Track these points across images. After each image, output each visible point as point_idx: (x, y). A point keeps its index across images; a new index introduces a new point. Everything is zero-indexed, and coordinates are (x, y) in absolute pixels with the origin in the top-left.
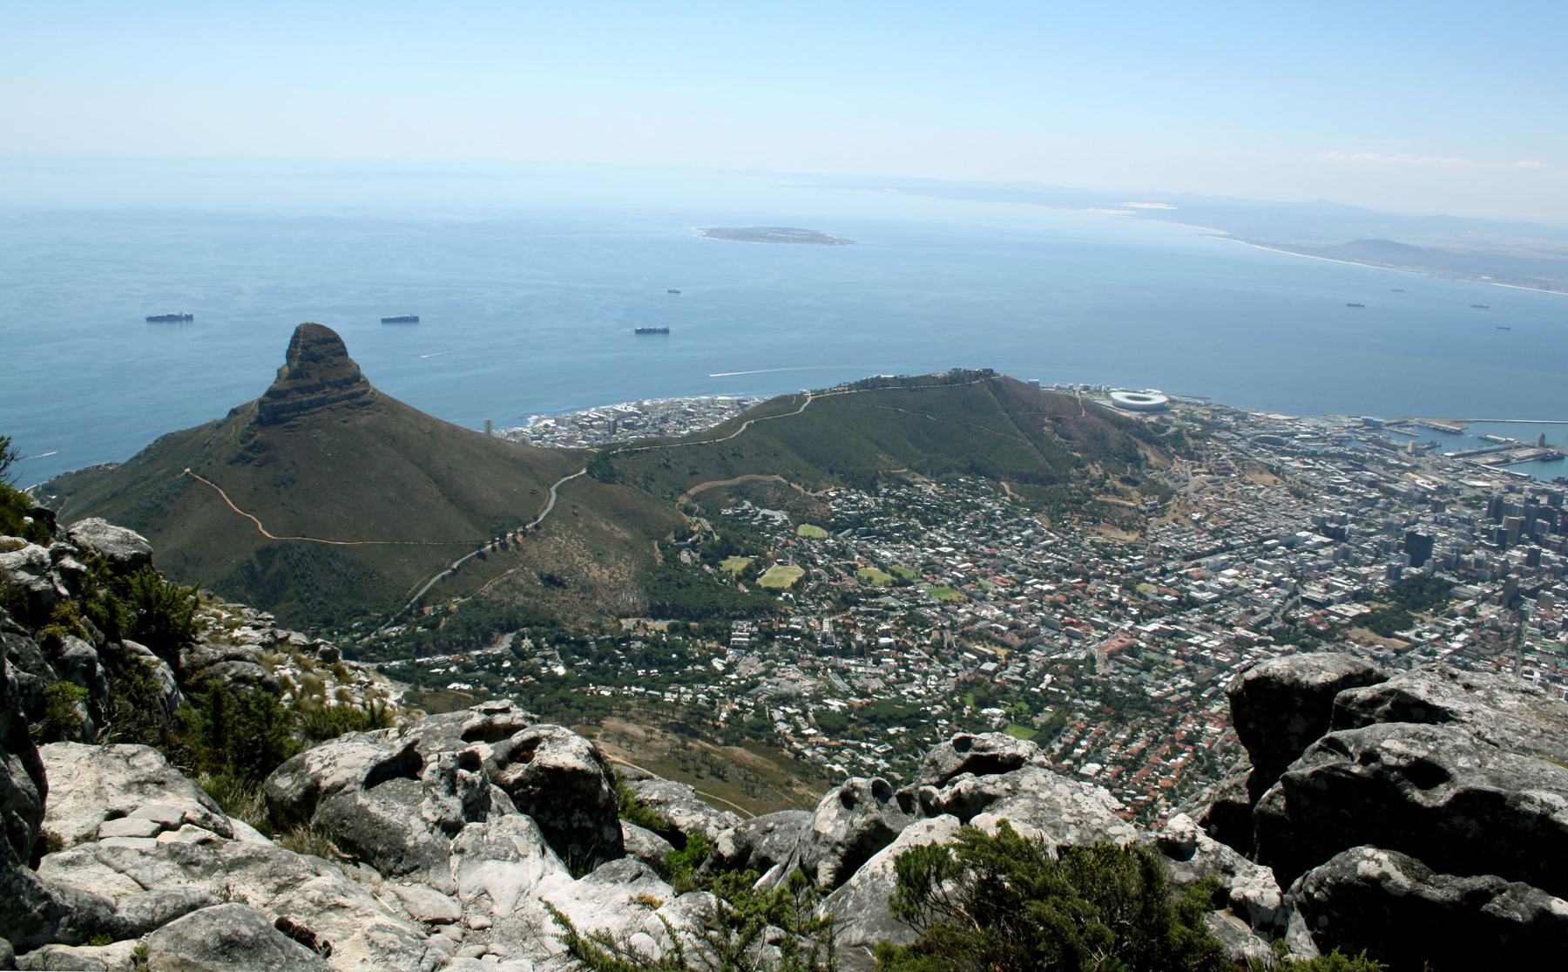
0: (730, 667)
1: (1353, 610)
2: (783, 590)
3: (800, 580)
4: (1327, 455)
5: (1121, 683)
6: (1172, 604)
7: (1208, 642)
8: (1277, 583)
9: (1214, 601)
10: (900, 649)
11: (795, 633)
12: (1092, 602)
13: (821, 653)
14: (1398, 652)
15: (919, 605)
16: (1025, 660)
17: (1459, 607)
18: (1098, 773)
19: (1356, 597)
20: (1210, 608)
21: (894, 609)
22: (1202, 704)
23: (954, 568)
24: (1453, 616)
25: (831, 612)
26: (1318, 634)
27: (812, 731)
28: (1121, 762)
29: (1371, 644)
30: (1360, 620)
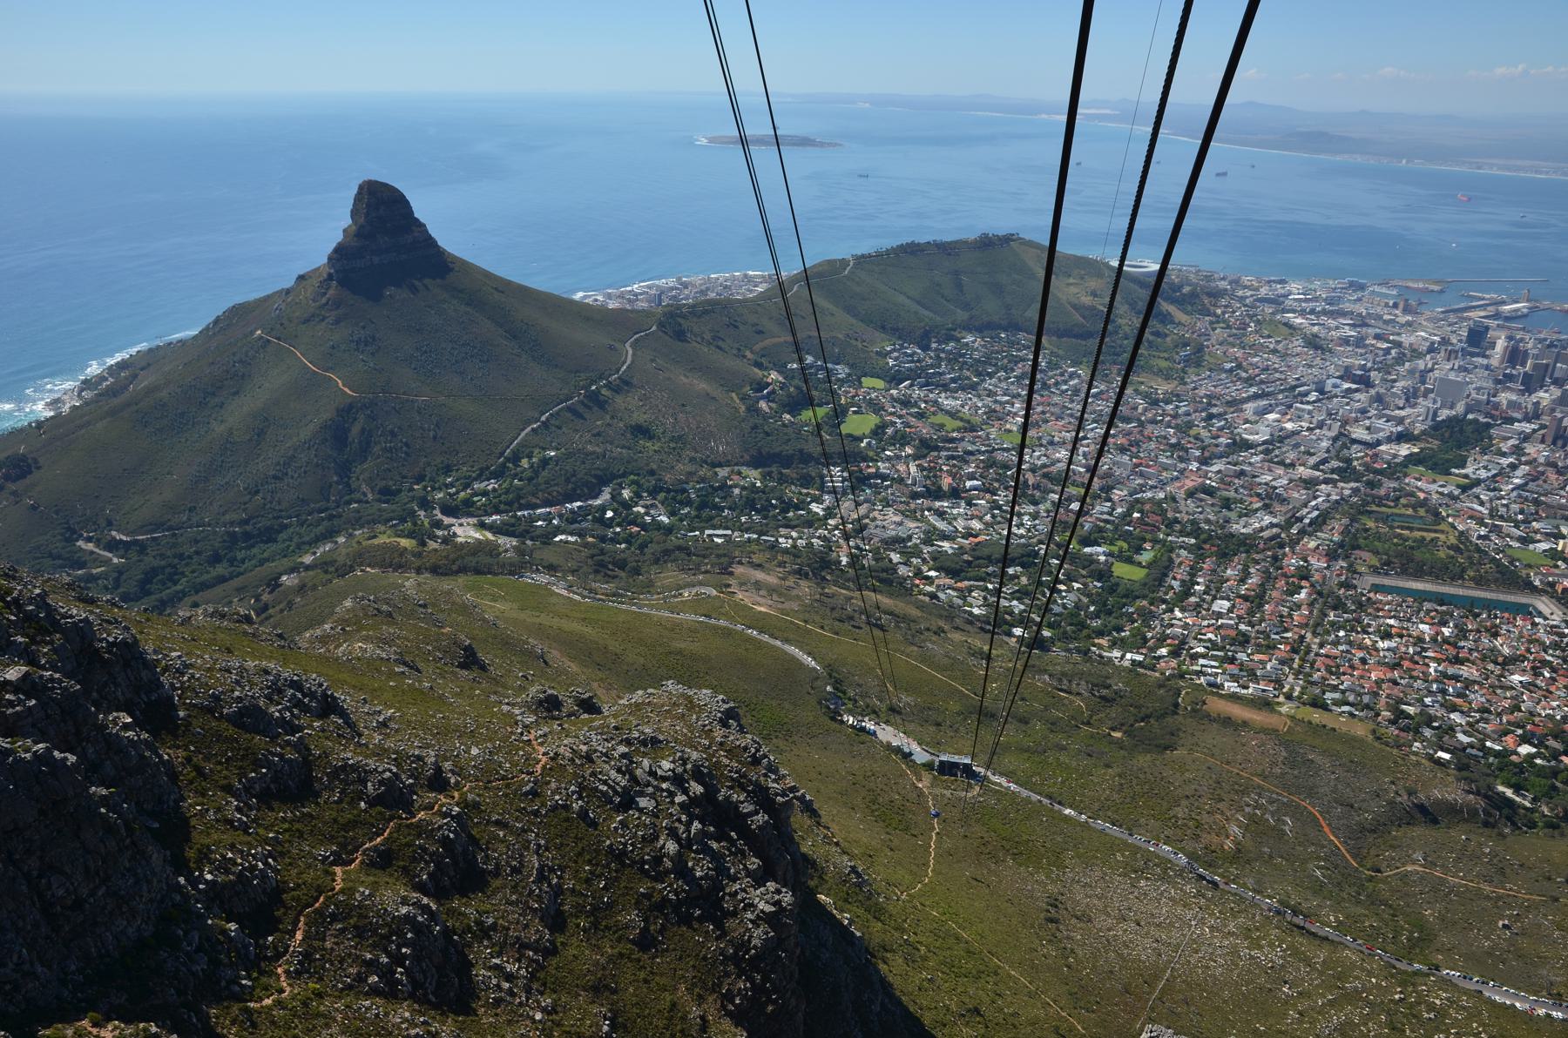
0: (830, 513)
1: (1404, 450)
2: (864, 436)
3: (878, 427)
4: (1324, 312)
5: (1208, 521)
6: (1228, 445)
7: (1278, 479)
8: (1321, 425)
9: (1265, 442)
10: (988, 491)
11: (884, 477)
12: (1153, 445)
13: (915, 496)
14: (1464, 488)
15: (994, 450)
16: (1110, 500)
17: (1505, 447)
18: (1230, 610)
19: (1401, 438)
20: (1269, 447)
21: (971, 453)
22: (1293, 543)
23: (1016, 414)
24: (1504, 455)
25: (915, 457)
26: (1377, 472)
27: (933, 573)
28: (1245, 598)
29: (1434, 481)
30: (1412, 459)
